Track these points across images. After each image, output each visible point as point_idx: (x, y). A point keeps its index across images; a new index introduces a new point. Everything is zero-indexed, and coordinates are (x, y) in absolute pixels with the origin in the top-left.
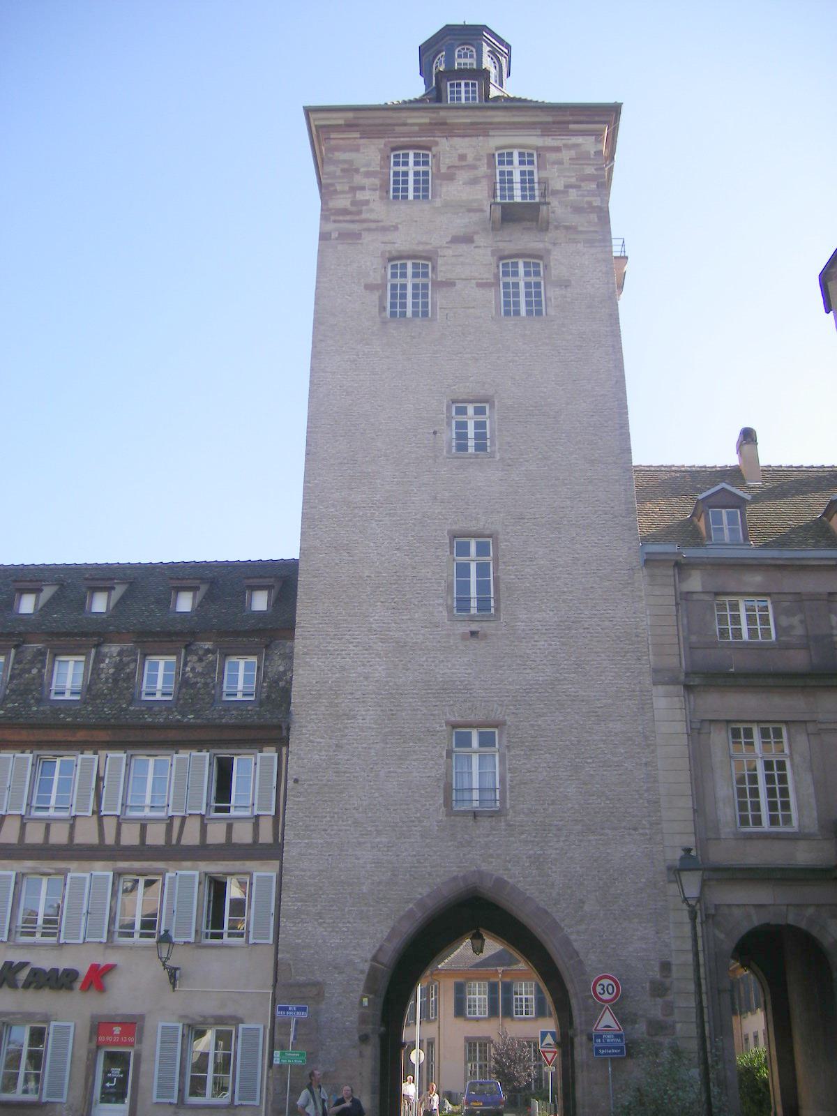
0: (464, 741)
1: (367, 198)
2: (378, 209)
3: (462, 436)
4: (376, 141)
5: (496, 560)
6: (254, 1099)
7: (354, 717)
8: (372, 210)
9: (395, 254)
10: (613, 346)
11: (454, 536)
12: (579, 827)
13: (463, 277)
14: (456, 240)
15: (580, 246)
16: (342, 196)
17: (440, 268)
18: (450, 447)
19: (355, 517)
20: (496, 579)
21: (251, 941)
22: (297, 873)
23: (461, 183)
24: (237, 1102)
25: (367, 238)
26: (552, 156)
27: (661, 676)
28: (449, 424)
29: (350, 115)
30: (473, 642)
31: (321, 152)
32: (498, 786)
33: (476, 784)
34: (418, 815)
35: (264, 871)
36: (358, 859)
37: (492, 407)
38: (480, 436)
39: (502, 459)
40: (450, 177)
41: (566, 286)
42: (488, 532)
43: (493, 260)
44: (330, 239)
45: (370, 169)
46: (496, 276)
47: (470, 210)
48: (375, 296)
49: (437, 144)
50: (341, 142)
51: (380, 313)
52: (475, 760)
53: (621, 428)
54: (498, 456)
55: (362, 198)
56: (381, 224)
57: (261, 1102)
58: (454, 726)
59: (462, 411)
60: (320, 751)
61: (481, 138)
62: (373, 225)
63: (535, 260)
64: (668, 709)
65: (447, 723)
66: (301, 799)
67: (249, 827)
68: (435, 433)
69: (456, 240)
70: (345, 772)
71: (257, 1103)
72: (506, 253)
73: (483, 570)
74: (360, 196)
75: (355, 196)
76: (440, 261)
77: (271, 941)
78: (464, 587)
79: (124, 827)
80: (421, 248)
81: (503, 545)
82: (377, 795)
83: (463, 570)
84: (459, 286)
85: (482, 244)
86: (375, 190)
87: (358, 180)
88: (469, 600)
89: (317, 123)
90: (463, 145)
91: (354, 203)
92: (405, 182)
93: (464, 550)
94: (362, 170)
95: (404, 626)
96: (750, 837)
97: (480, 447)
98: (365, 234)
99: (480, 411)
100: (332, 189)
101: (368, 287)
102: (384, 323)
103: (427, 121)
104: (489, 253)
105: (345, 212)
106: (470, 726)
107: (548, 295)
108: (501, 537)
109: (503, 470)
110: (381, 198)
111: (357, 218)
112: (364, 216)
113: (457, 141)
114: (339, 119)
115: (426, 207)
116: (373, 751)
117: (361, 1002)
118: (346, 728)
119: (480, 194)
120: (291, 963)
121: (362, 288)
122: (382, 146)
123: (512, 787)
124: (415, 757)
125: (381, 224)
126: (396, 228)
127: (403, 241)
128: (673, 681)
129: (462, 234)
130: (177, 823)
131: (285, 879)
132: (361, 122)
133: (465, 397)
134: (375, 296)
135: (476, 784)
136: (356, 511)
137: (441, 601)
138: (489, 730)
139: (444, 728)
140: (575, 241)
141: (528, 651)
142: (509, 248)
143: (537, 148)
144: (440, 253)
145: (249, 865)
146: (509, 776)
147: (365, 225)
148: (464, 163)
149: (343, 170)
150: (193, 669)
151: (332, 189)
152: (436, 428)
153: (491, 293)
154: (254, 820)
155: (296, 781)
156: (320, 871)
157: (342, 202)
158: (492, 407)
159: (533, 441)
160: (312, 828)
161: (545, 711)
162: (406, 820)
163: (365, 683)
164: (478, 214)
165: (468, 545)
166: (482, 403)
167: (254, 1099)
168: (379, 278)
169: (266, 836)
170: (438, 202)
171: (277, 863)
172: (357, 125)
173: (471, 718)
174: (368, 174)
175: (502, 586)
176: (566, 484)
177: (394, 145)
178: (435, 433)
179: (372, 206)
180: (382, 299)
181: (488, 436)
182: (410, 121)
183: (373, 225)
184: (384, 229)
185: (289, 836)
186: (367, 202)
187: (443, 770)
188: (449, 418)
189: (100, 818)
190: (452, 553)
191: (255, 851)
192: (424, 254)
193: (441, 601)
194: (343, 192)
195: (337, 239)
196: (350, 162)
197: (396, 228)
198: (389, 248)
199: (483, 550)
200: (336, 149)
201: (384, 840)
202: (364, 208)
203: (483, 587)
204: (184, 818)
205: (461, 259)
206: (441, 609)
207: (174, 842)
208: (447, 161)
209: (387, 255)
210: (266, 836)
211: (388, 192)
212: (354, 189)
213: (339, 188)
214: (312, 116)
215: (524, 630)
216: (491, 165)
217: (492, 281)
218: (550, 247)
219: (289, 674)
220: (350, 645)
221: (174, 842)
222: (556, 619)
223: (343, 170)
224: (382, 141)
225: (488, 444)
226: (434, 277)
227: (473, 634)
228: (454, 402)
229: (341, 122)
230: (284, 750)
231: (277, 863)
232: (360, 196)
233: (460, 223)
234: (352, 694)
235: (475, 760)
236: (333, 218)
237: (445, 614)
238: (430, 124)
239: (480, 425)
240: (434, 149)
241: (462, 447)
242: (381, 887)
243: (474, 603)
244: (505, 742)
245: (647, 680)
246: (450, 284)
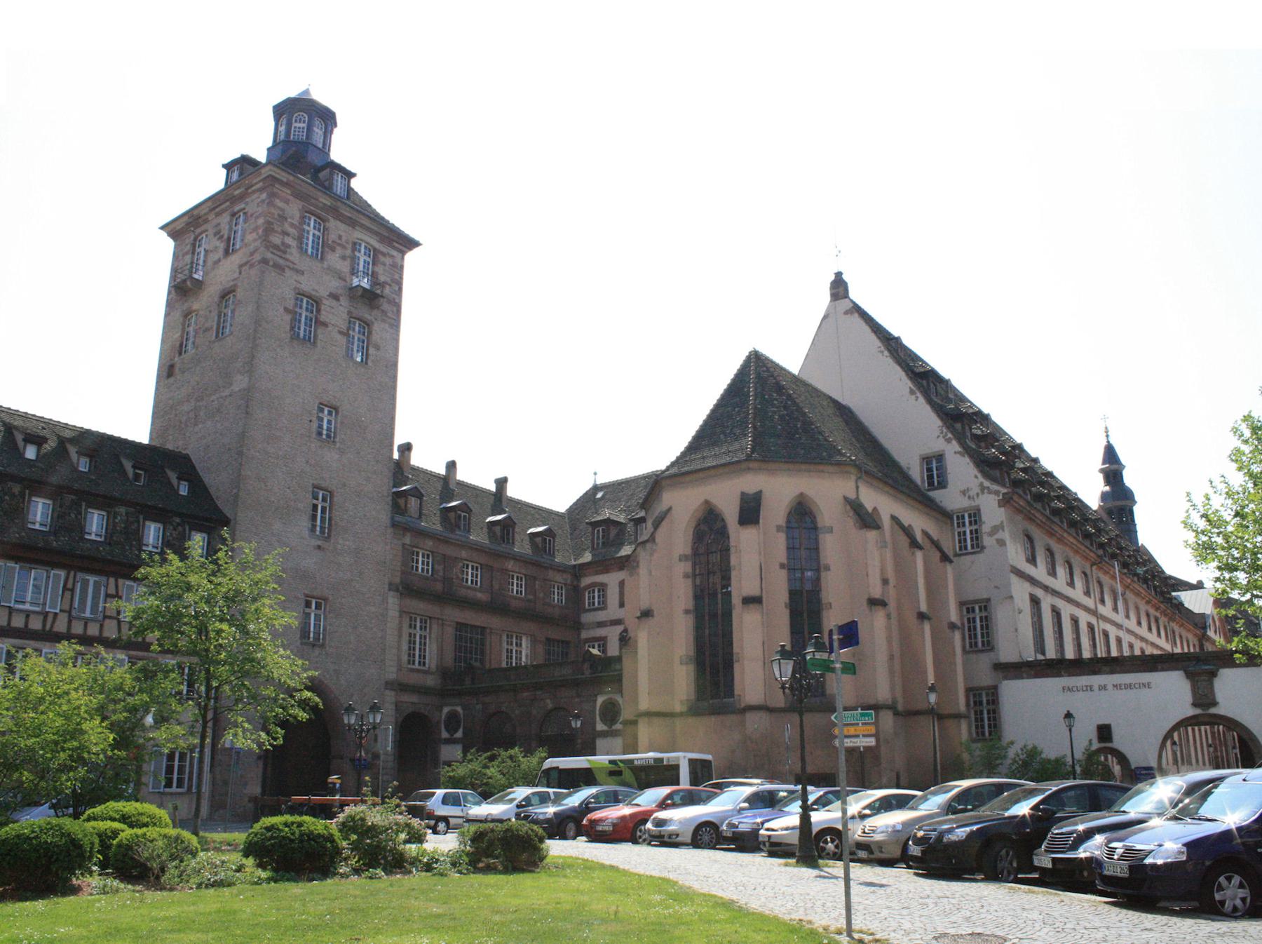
3: (321, 427)
17: (323, 312)
25: (288, 273)
26: (382, 259)
27: (392, 587)
37: (337, 413)
40: (333, 250)
59: (322, 411)
63: (366, 325)
64: (393, 601)
73: (324, 509)
74: (288, 240)
96: (412, 670)
97: (328, 436)
101: (286, 309)
102: (292, 338)
105: (276, 247)
112: (288, 256)
113: (339, 223)
126: (303, 273)
127: (307, 284)
128: (397, 590)
142: (356, 313)
143: (375, 249)
157: (276, 239)
158: (337, 413)
166: (334, 409)
170: (325, 265)
174: (292, 225)
184: (297, 271)
186: (289, 246)
196: (283, 210)
197: (303, 273)
212: (285, 233)
213: (276, 227)
216: (354, 250)
233: (334, 285)
241: (320, 434)
246: (325, 325)
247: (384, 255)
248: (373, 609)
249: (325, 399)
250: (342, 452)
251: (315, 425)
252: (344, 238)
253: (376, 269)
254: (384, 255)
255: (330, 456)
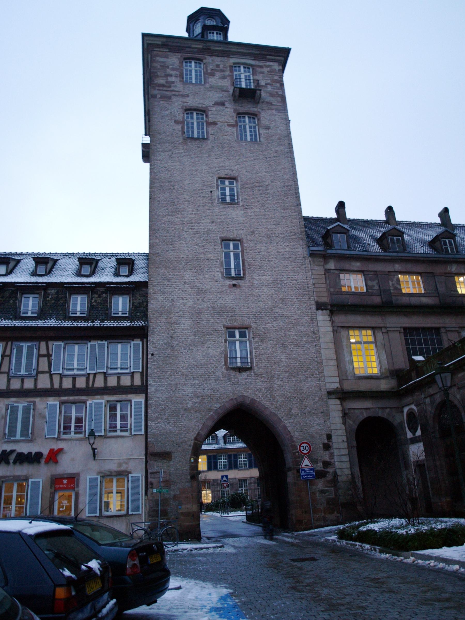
0: (232, 335)
1: (173, 80)
2: (179, 86)
3: (224, 194)
4: (177, 54)
5: (242, 251)
6: (139, 511)
7: (179, 324)
8: (176, 86)
9: (188, 107)
10: (291, 158)
11: (223, 240)
12: (287, 374)
13: (221, 121)
14: (217, 104)
15: (274, 111)
16: (161, 78)
18: (219, 199)
19: (175, 229)
20: (243, 261)
21: (133, 433)
22: (154, 399)
23: (218, 77)
24: (130, 513)
25: (174, 99)
28: (217, 188)
29: (164, 40)
30: (234, 289)
31: (148, 57)
32: (249, 356)
33: (238, 355)
34: (213, 370)
35: (139, 399)
36: (185, 392)
37: (237, 181)
38: (232, 195)
39: (243, 206)
41: (268, 129)
42: (238, 239)
43: (235, 115)
44: (156, 98)
45: (174, 67)
46: (236, 122)
47: (223, 91)
48: (179, 127)
49: (205, 58)
50: (160, 53)
51: (182, 134)
52: (238, 344)
53: (296, 194)
54: (241, 204)
55: (171, 80)
56: (180, 93)
57: (142, 512)
58: (228, 328)
60: (164, 340)
61: (226, 58)
62: (177, 93)
65: (224, 326)
66: (155, 363)
67: (129, 378)
68: (211, 192)
69: (217, 104)
70: (176, 350)
71: (140, 512)
72: (240, 112)
73: (236, 256)
74: (170, 79)
75: (167, 79)
76: (210, 113)
77: (143, 433)
78: (228, 264)
79: (64, 379)
80: (200, 106)
81: (245, 245)
82: (192, 361)
83: (227, 256)
84: (219, 125)
85: (228, 107)
86: (177, 77)
87: (169, 71)
88: (230, 270)
89: (148, 42)
90: (218, 60)
91: (167, 82)
92: (191, 75)
93: (227, 247)
94: (170, 67)
95: (201, 281)
97: (232, 200)
98: (173, 97)
99: (231, 183)
100: (156, 74)
103: (201, 47)
104: (232, 111)
106: (235, 328)
107: (261, 132)
108: (244, 241)
109: (244, 210)
110: (180, 81)
111: (169, 89)
112: (172, 88)
114: (158, 41)
115: (202, 87)
116: (189, 340)
117: (190, 460)
118: (176, 329)
119: (227, 83)
120: (155, 443)
121: (173, 122)
122: (179, 57)
123: (256, 356)
124: (209, 343)
125: (180, 93)
126: (188, 96)
127: (192, 102)
129: (219, 101)
130: (91, 377)
131: (149, 402)
132: (170, 44)
133: (225, 176)
134: (179, 127)
135: (238, 355)
136: (175, 226)
137: (218, 270)
138: (244, 330)
139: (223, 329)
140: (272, 109)
141: (260, 294)
144: (210, 109)
145: (130, 397)
146: (254, 351)
147: (174, 93)
148: (218, 69)
149: (161, 66)
150: (96, 301)
151: (156, 74)
152: (212, 190)
153: (234, 129)
154: (131, 374)
155: (152, 355)
156: (167, 398)
159: (257, 198)
160: (161, 377)
161: (269, 321)
162: (207, 372)
163: (184, 308)
164: (226, 93)
165: (229, 245)
167: (139, 511)
168: (181, 118)
169: (137, 381)
171: (144, 395)
172: (168, 45)
173: (235, 324)
174: (173, 69)
175: (246, 263)
176: (273, 218)
177: (185, 57)
178: (211, 192)
179: (176, 84)
180: (183, 128)
181: (236, 194)
182: (193, 46)
183: (177, 93)
184: (183, 96)
185: (150, 381)
186: (173, 82)
187: (223, 349)
188: (218, 186)
189: (51, 375)
190: (222, 248)
191: (132, 390)
192: (202, 109)
193: (218, 270)
194: (161, 76)
195: (159, 98)
198: (185, 104)
199: (236, 247)
200: (157, 55)
201: (197, 382)
202: (172, 85)
203: (237, 264)
204: (95, 374)
205: (220, 113)
206: (218, 273)
207: (90, 386)
208: (211, 67)
209: (184, 108)
210: (137, 381)
211: (183, 78)
214: (146, 38)
215: (257, 284)
217: (234, 124)
218: (260, 111)
219: (145, 304)
220: (176, 290)
221: (90, 386)
222: (272, 279)
223: (161, 66)
224: (180, 54)
225: (236, 198)
226: (207, 120)
227: (234, 285)
228: (220, 178)
229: (160, 43)
230: (145, 340)
231: (144, 395)
232: (170, 79)
234: (177, 313)
235: (238, 344)
236: (157, 88)
237: (220, 276)
238: (203, 48)
239: (231, 190)
240: (204, 61)
241: (224, 200)
242: (197, 405)
243: (233, 271)
244: (251, 335)
245: (314, 307)
246: (215, 124)
247: (261, 67)
248: (302, 329)
249: (223, 173)
250: (245, 208)
251: (217, 193)
252: (221, 66)
253: (256, 77)
254: (261, 67)
255: (235, 213)
